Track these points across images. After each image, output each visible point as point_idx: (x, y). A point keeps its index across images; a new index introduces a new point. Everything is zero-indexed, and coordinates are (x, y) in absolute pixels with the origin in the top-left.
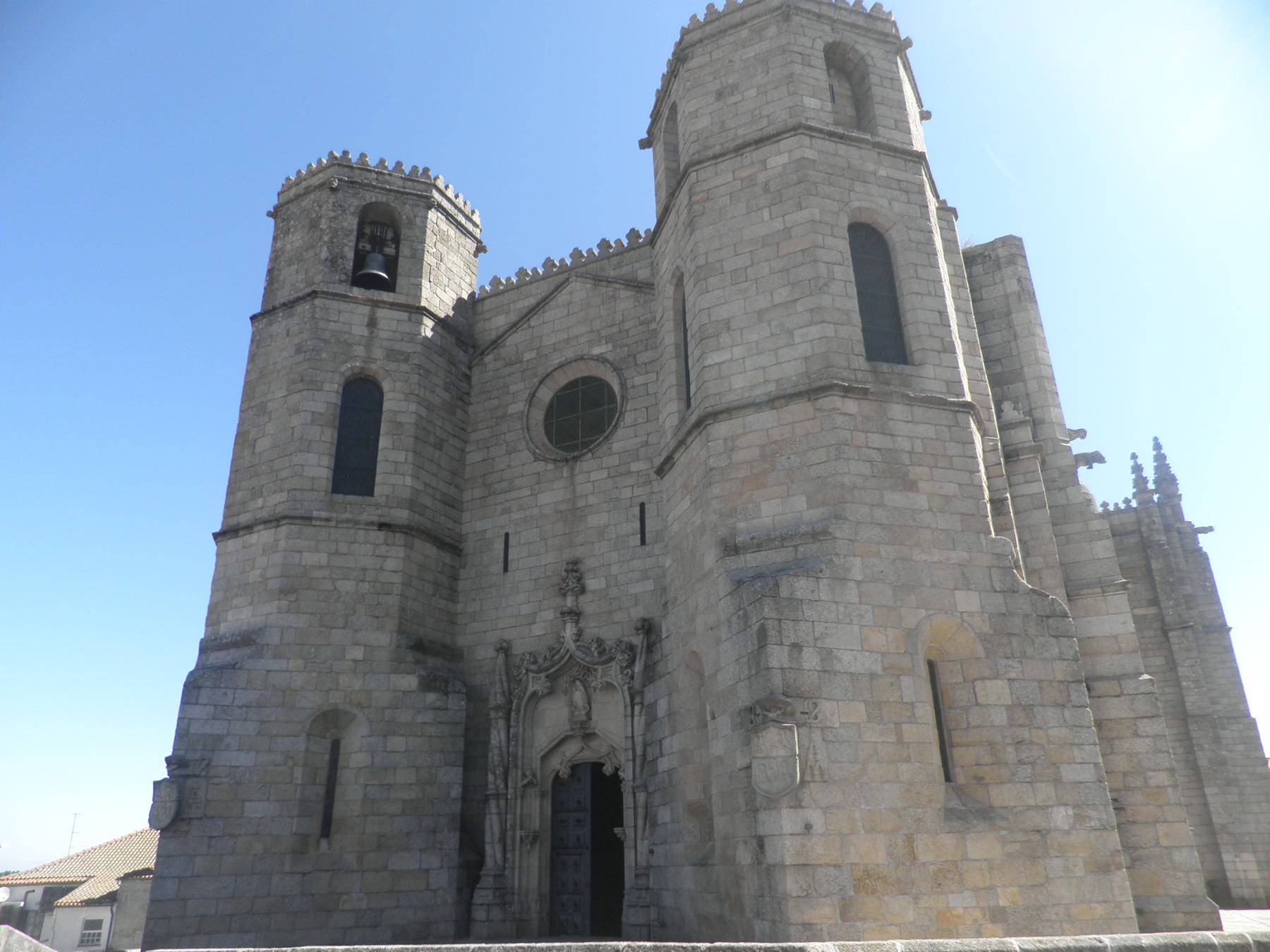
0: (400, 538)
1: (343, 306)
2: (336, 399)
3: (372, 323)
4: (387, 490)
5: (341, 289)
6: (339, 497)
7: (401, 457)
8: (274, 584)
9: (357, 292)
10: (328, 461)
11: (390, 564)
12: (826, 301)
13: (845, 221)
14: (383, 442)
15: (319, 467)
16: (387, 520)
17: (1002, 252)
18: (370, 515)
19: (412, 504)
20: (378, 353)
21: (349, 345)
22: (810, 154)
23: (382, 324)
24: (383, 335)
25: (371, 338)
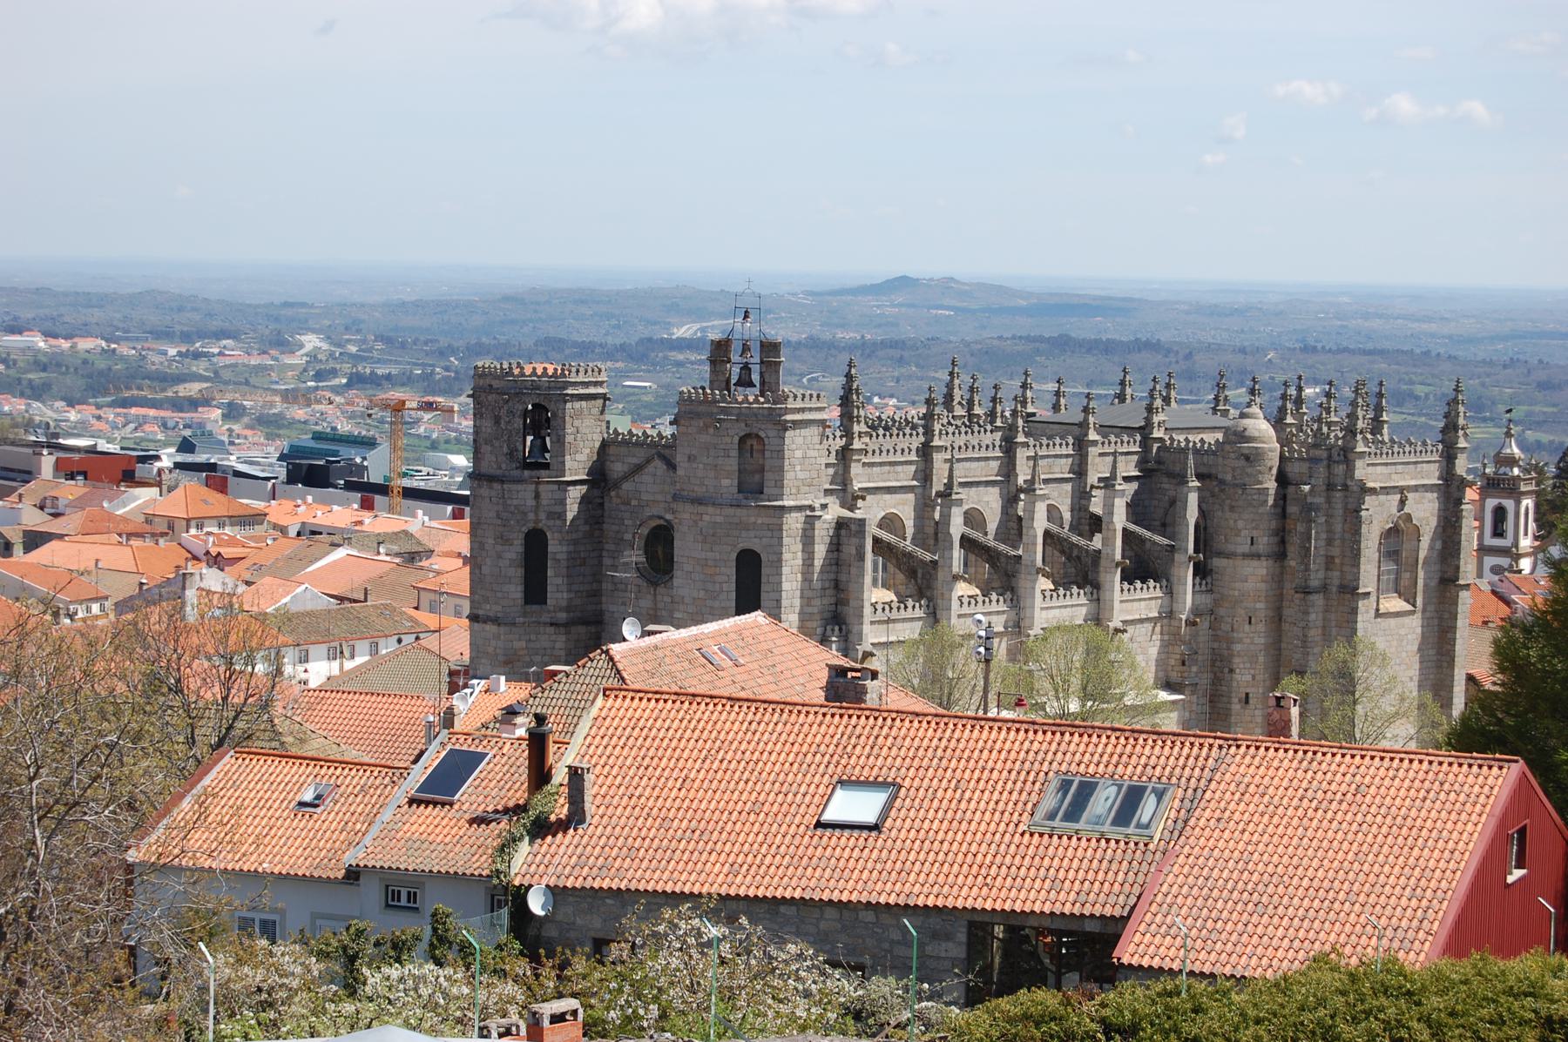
0: (562, 630)
1: (520, 487)
2: (521, 549)
3: (537, 496)
4: (554, 602)
5: (517, 473)
6: (528, 608)
7: (559, 581)
8: (501, 658)
9: (527, 473)
10: (521, 588)
11: (558, 645)
12: (717, 604)
13: (734, 556)
14: (550, 573)
15: (516, 591)
16: (554, 621)
17: (853, 527)
18: (545, 618)
19: (568, 609)
20: (542, 516)
21: (525, 514)
22: (719, 519)
23: (543, 495)
24: (544, 502)
25: (537, 507)
